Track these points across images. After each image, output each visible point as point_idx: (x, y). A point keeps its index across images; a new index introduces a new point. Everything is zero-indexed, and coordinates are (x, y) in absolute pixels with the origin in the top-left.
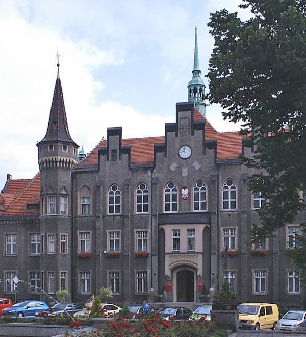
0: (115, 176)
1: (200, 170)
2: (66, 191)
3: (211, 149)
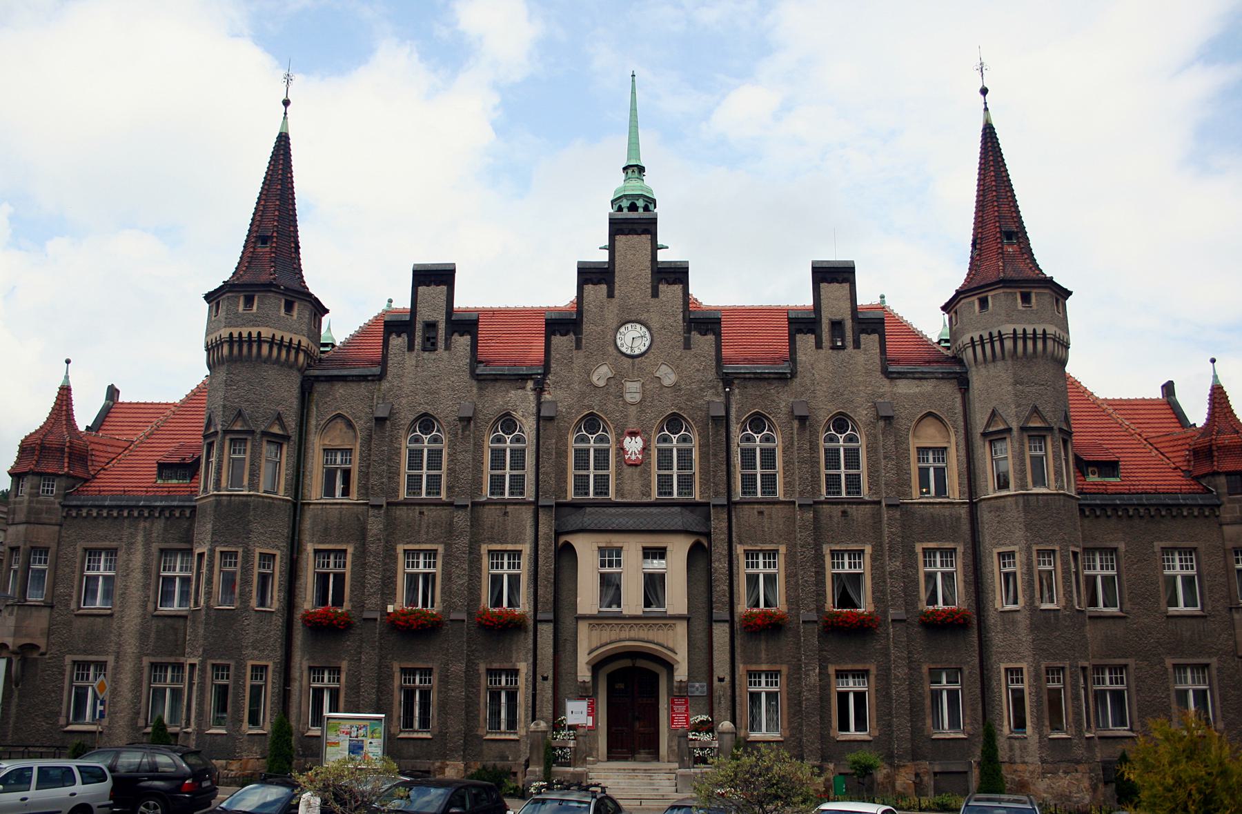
0: (429, 392)
1: (675, 387)
2: (283, 427)
3: (705, 335)
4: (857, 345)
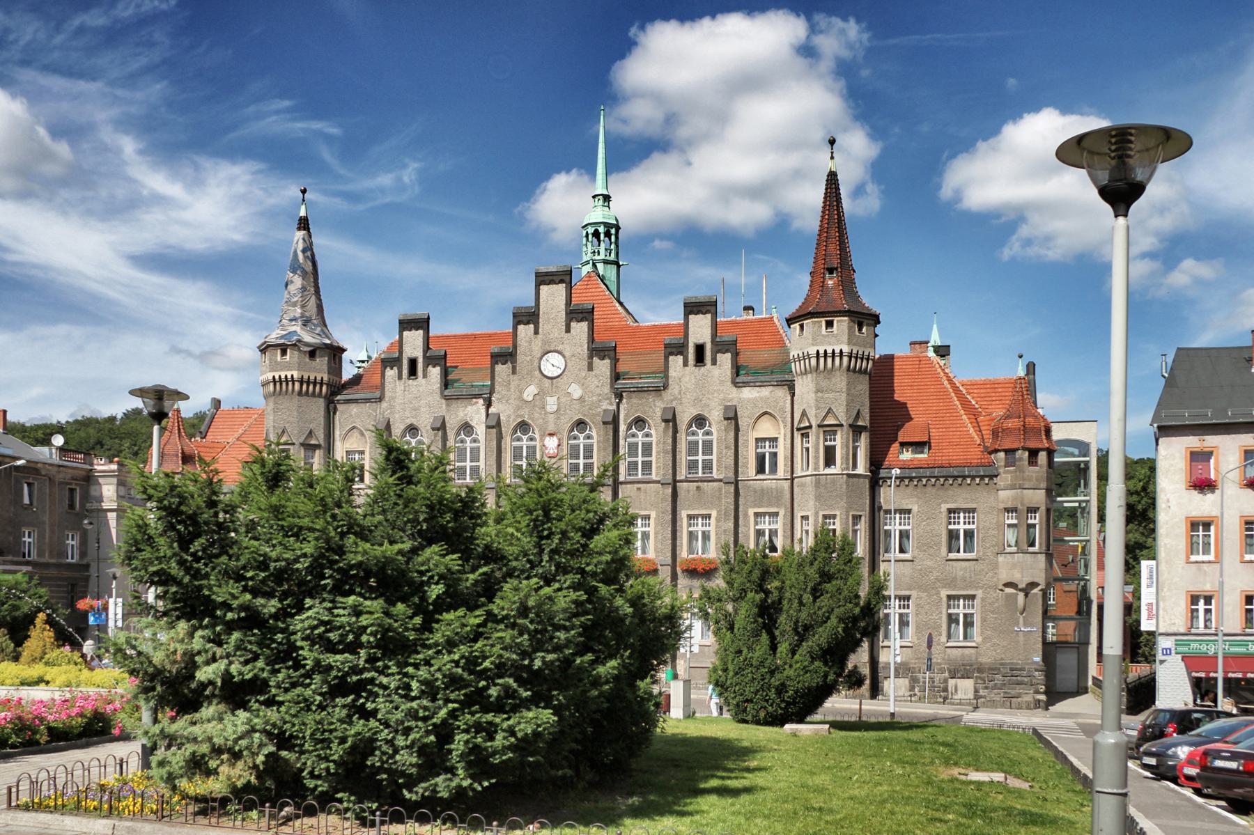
1: (581, 399)
4: (714, 362)
